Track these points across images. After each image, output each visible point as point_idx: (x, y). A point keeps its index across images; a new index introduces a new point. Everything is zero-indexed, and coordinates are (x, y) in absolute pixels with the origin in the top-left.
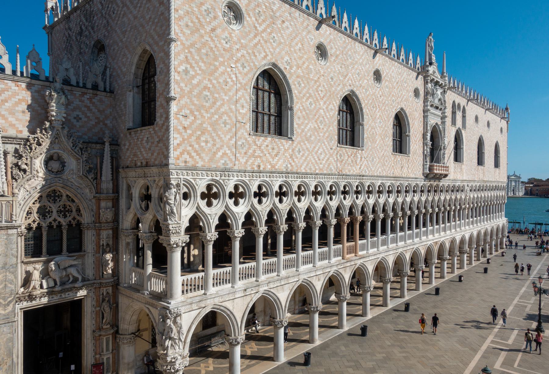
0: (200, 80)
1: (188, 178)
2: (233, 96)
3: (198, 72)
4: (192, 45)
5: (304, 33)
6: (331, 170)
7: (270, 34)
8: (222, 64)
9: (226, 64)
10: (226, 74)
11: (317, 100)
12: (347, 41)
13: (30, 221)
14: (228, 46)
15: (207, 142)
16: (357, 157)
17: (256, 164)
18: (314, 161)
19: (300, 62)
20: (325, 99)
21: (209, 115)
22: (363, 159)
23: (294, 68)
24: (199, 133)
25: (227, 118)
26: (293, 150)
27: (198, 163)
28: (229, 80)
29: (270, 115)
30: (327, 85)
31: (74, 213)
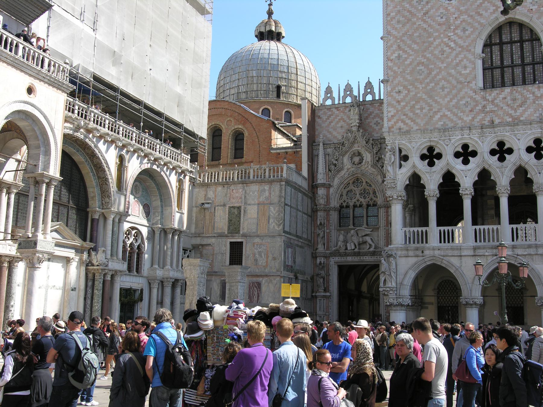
0: (413, 59)
1: (404, 142)
2: (452, 61)
3: (411, 53)
4: (403, 35)
9: (442, 36)
10: (442, 44)
13: (342, 201)
14: (444, 20)
15: (422, 109)
17: (488, 119)
21: (423, 86)
24: (414, 102)
25: (445, 83)
27: (412, 128)
28: (446, 49)
29: (523, 65)
31: (371, 195)
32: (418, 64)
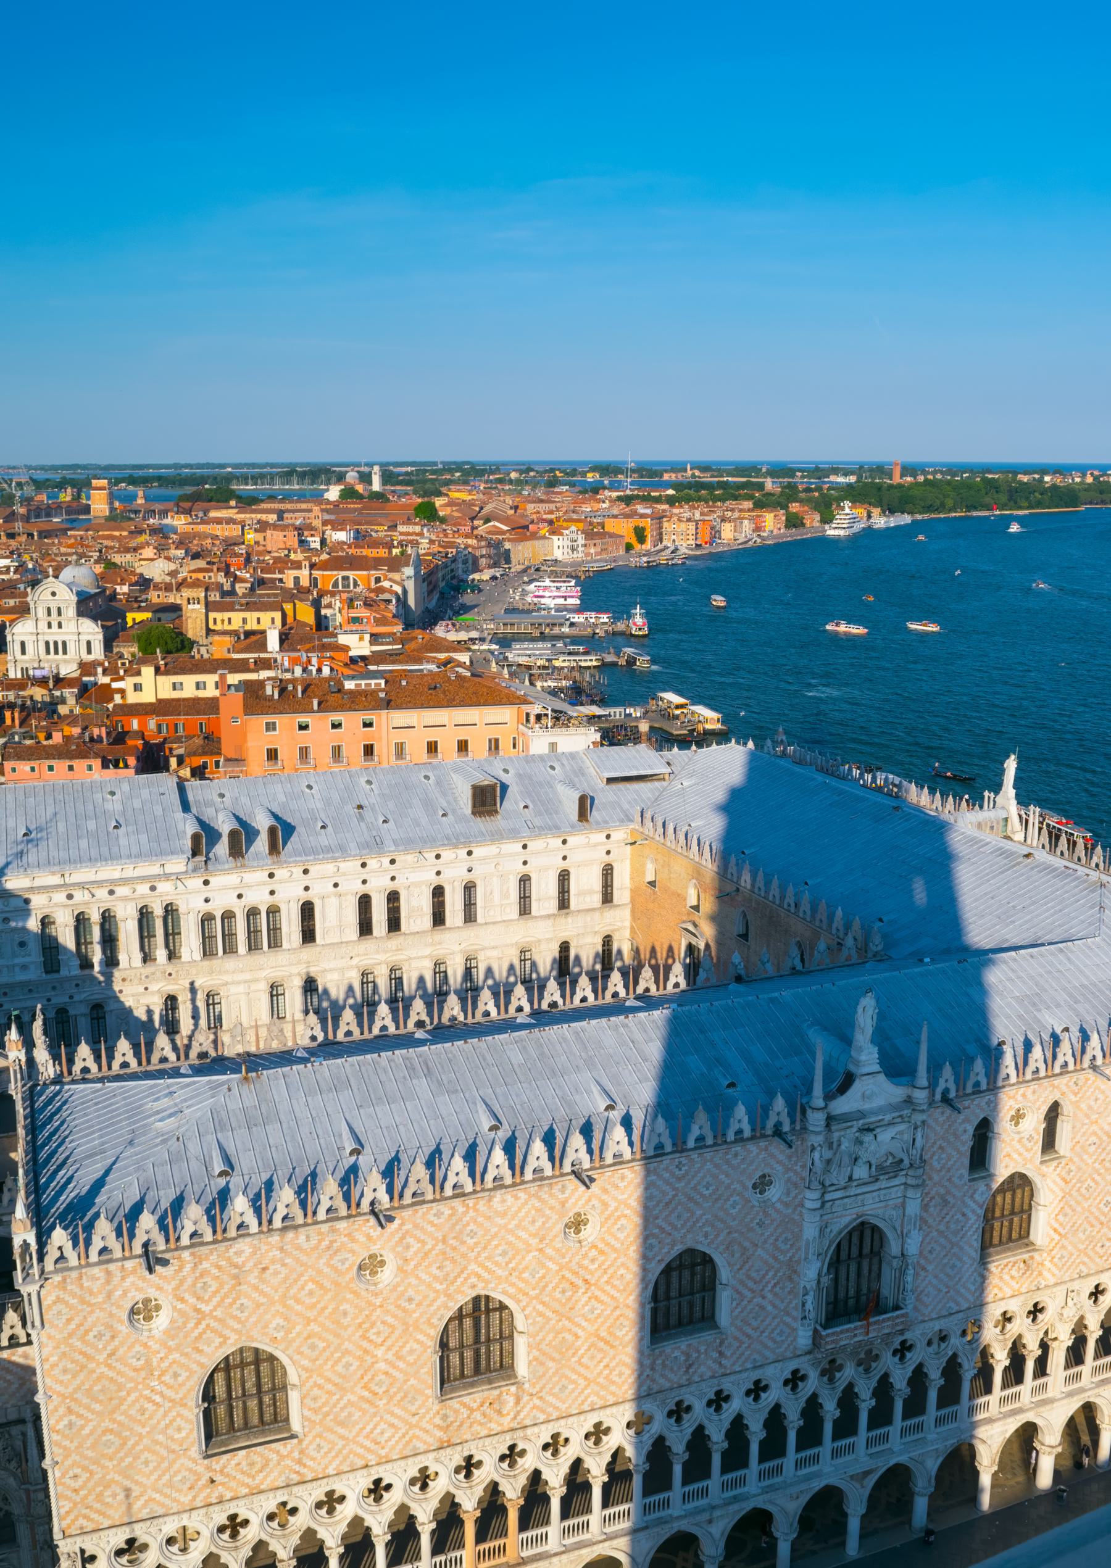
2: (158, 1423)
3: (90, 1416)
4: (75, 1391)
5: (323, 1261)
6: (415, 1448)
7: (231, 1305)
8: (135, 1389)
11: (366, 1351)
12: (461, 1209)
14: (142, 1362)
15: (114, 1496)
16: (503, 1403)
18: (361, 1451)
19: (311, 1314)
20: (389, 1343)
22: (526, 1398)
23: (298, 1328)
26: (302, 1452)
30: (395, 1316)
32: (104, 1432)
